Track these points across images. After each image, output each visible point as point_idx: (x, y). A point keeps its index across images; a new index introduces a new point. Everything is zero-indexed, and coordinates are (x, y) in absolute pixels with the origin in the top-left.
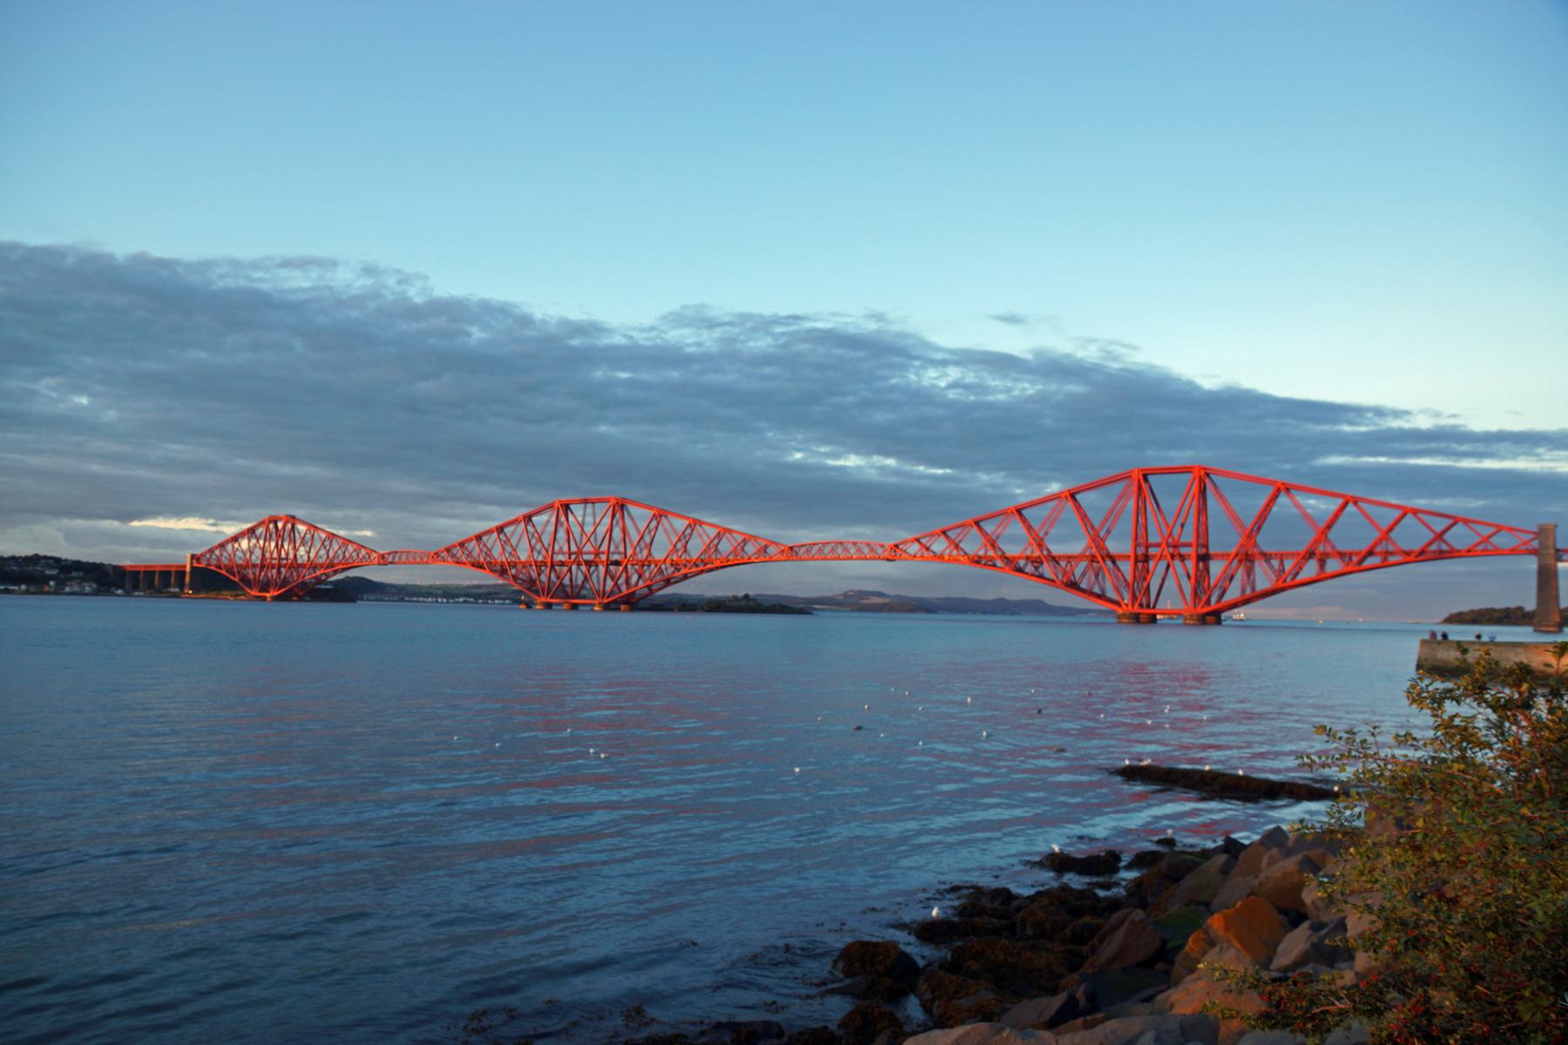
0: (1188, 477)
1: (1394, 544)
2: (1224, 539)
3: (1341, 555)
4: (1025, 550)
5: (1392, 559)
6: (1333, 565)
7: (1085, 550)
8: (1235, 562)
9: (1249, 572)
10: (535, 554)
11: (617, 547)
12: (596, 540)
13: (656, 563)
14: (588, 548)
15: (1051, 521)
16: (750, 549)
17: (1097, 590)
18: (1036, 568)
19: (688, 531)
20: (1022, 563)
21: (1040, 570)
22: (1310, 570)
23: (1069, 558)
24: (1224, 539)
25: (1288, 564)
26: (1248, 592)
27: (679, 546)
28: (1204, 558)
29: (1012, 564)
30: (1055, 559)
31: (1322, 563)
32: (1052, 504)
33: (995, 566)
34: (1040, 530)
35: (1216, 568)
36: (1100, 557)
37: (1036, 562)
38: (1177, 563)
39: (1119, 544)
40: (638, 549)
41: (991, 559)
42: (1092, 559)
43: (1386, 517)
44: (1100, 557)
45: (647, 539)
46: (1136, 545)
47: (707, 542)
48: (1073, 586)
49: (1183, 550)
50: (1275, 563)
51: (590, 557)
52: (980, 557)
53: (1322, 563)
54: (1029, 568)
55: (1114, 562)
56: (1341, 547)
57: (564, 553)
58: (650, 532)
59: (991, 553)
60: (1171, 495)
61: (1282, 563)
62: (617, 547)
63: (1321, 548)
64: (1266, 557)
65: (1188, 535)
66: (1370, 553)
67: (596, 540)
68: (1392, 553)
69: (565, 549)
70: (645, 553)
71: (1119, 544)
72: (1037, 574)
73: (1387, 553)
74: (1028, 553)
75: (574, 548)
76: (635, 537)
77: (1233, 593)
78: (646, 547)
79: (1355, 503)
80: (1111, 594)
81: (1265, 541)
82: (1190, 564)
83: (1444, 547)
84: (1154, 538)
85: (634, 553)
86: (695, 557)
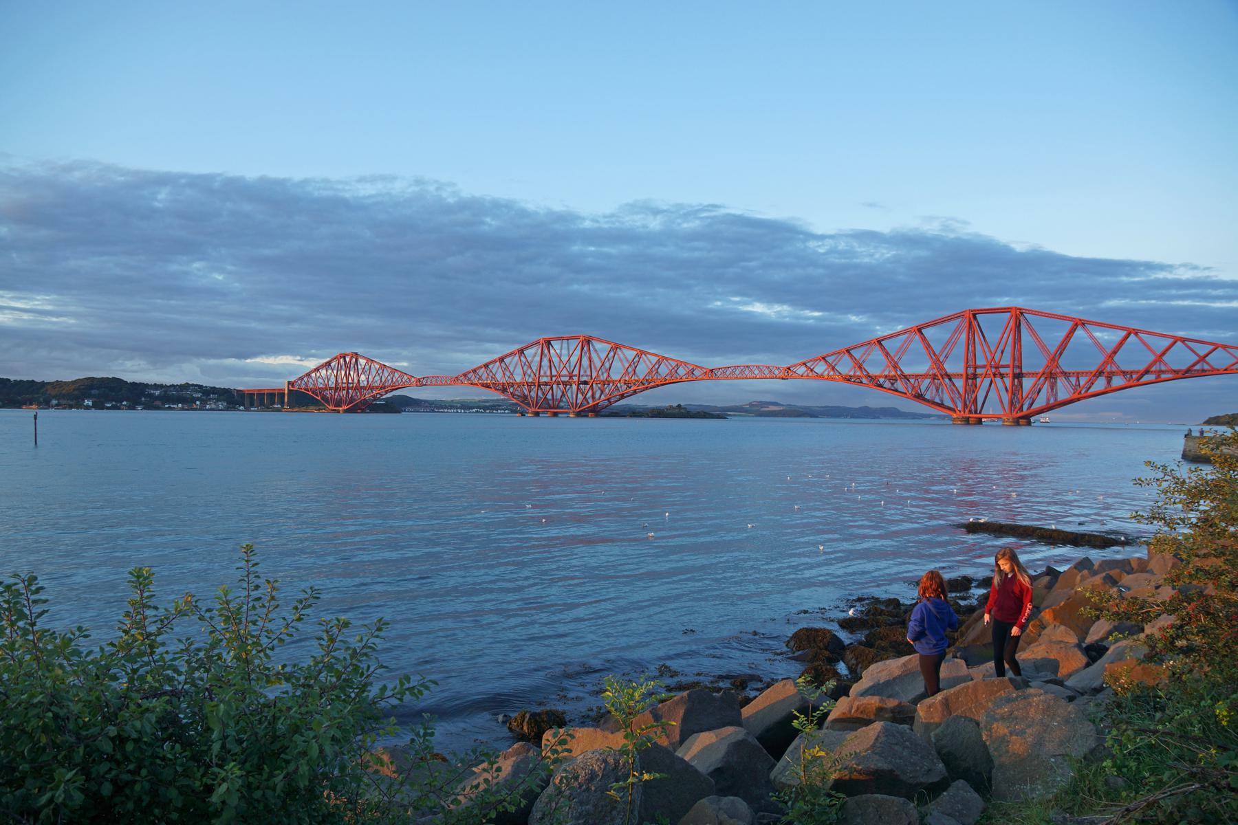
0: (1007, 315)
1: (1166, 364)
2: (1033, 361)
3: (1124, 373)
4: (884, 370)
5: (1163, 376)
6: (1117, 381)
7: (929, 370)
8: (1042, 379)
9: (1053, 386)
10: (527, 377)
11: (585, 372)
12: (570, 366)
13: (614, 382)
14: (565, 372)
15: (903, 350)
16: (682, 371)
17: (937, 400)
18: (892, 384)
19: (637, 359)
20: (881, 380)
21: (895, 385)
22: (1100, 384)
23: (917, 377)
24: (1033, 361)
25: (1083, 381)
26: (1052, 401)
27: (630, 369)
28: (1019, 376)
29: (875, 382)
30: (906, 377)
31: (1109, 380)
32: (904, 337)
33: (861, 382)
34: (895, 356)
35: (1027, 383)
36: (940, 375)
38: (998, 380)
39: (954, 366)
40: (600, 373)
41: (859, 377)
42: (934, 377)
44: (940, 375)
45: (607, 365)
46: (967, 367)
47: (651, 367)
48: (920, 397)
49: (1002, 370)
50: (1073, 380)
51: (566, 379)
52: (850, 376)
53: (1109, 380)
54: (888, 384)
55: (950, 380)
56: (1124, 368)
57: (547, 376)
58: (609, 360)
59: (858, 373)
60: (994, 330)
62: (585, 372)
63: (1108, 368)
64: (1066, 375)
65: (1007, 359)
66: (1147, 372)
67: (570, 366)
69: (548, 373)
70: (605, 375)
71: (954, 366)
74: (886, 373)
75: (554, 373)
76: (598, 364)
77: (1040, 402)
78: (606, 370)
79: (1136, 334)
80: (948, 403)
81: (1065, 364)
82: (1008, 381)
83: (1206, 367)
86: (641, 377)
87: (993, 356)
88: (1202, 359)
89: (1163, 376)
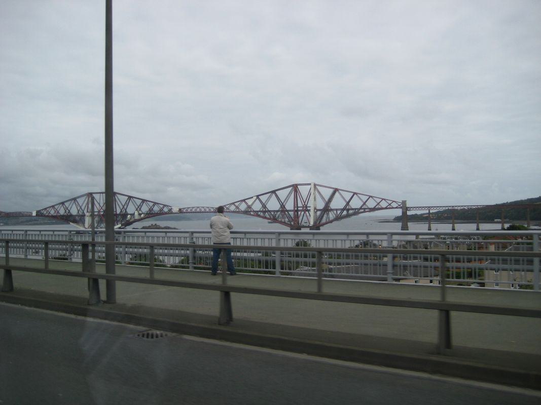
3: (353, 209)
5: (366, 210)
9: (328, 214)
14: (102, 210)
22: (345, 213)
25: (339, 212)
30: (270, 211)
36: (283, 210)
37: (264, 212)
43: (364, 198)
44: (283, 210)
45: (125, 207)
46: (294, 208)
64: (332, 210)
66: (361, 208)
68: (366, 209)
71: (290, 206)
73: (365, 209)
81: (333, 205)
84: (300, 204)
85: (121, 211)
87: (305, 204)
88: (378, 204)
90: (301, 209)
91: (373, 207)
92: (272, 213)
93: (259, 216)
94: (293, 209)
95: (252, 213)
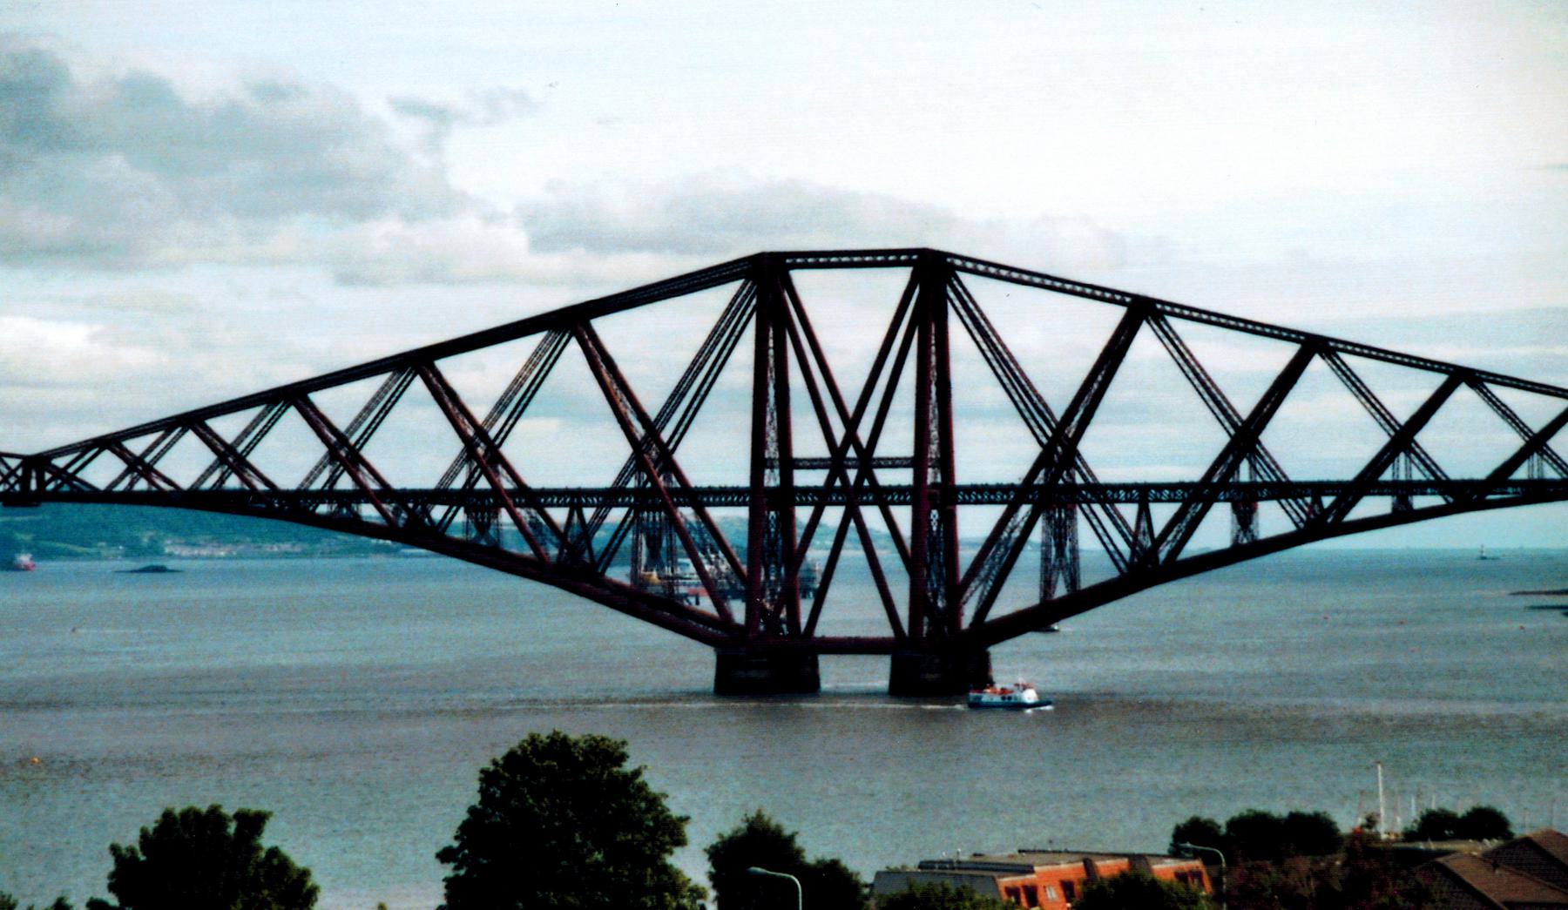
1: (1428, 464)
3: (1283, 490)
4: (451, 474)
5: (1419, 502)
6: (1272, 519)
8: (1025, 509)
9: (1061, 534)
23: (574, 498)
25: (1162, 514)
26: (1061, 590)
30: (538, 499)
31: (1245, 516)
35: (974, 523)
37: (480, 505)
38: (872, 516)
46: (759, 463)
49: (886, 477)
50: (1129, 511)
53: (1245, 516)
59: (345, 483)
61: (1144, 513)
63: (1244, 473)
64: (1106, 494)
65: (898, 439)
68: (1420, 488)
72: (483, 543)
73: (1403, 490)
77: (1019, 594)
82: (903, 515)
84: (808, 440)
87: (851, 424)
89: (1419, 502)
90: (817, 478)
91: (1480, 470)
92: (559, 515)
93: (436, 540)
94: (740, 477)
95: (368, 511)
